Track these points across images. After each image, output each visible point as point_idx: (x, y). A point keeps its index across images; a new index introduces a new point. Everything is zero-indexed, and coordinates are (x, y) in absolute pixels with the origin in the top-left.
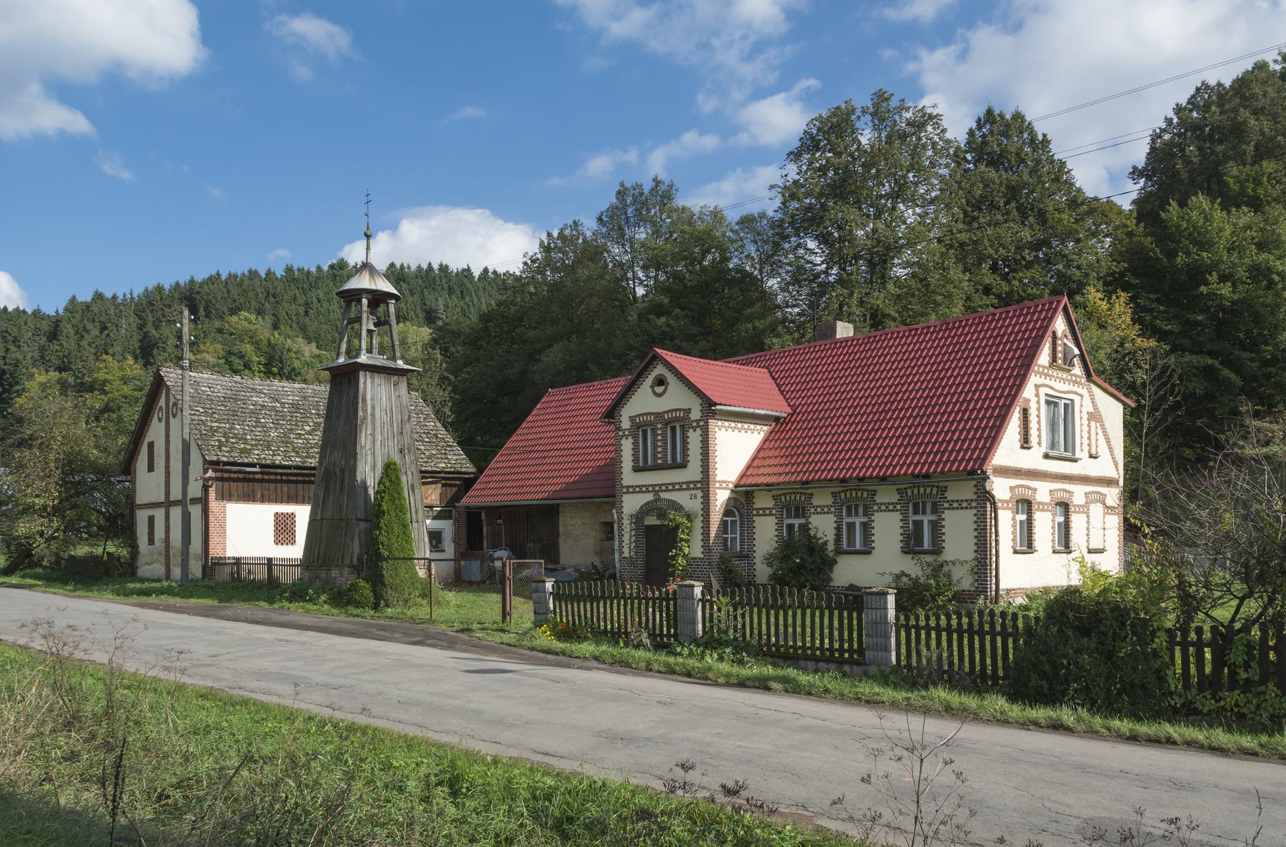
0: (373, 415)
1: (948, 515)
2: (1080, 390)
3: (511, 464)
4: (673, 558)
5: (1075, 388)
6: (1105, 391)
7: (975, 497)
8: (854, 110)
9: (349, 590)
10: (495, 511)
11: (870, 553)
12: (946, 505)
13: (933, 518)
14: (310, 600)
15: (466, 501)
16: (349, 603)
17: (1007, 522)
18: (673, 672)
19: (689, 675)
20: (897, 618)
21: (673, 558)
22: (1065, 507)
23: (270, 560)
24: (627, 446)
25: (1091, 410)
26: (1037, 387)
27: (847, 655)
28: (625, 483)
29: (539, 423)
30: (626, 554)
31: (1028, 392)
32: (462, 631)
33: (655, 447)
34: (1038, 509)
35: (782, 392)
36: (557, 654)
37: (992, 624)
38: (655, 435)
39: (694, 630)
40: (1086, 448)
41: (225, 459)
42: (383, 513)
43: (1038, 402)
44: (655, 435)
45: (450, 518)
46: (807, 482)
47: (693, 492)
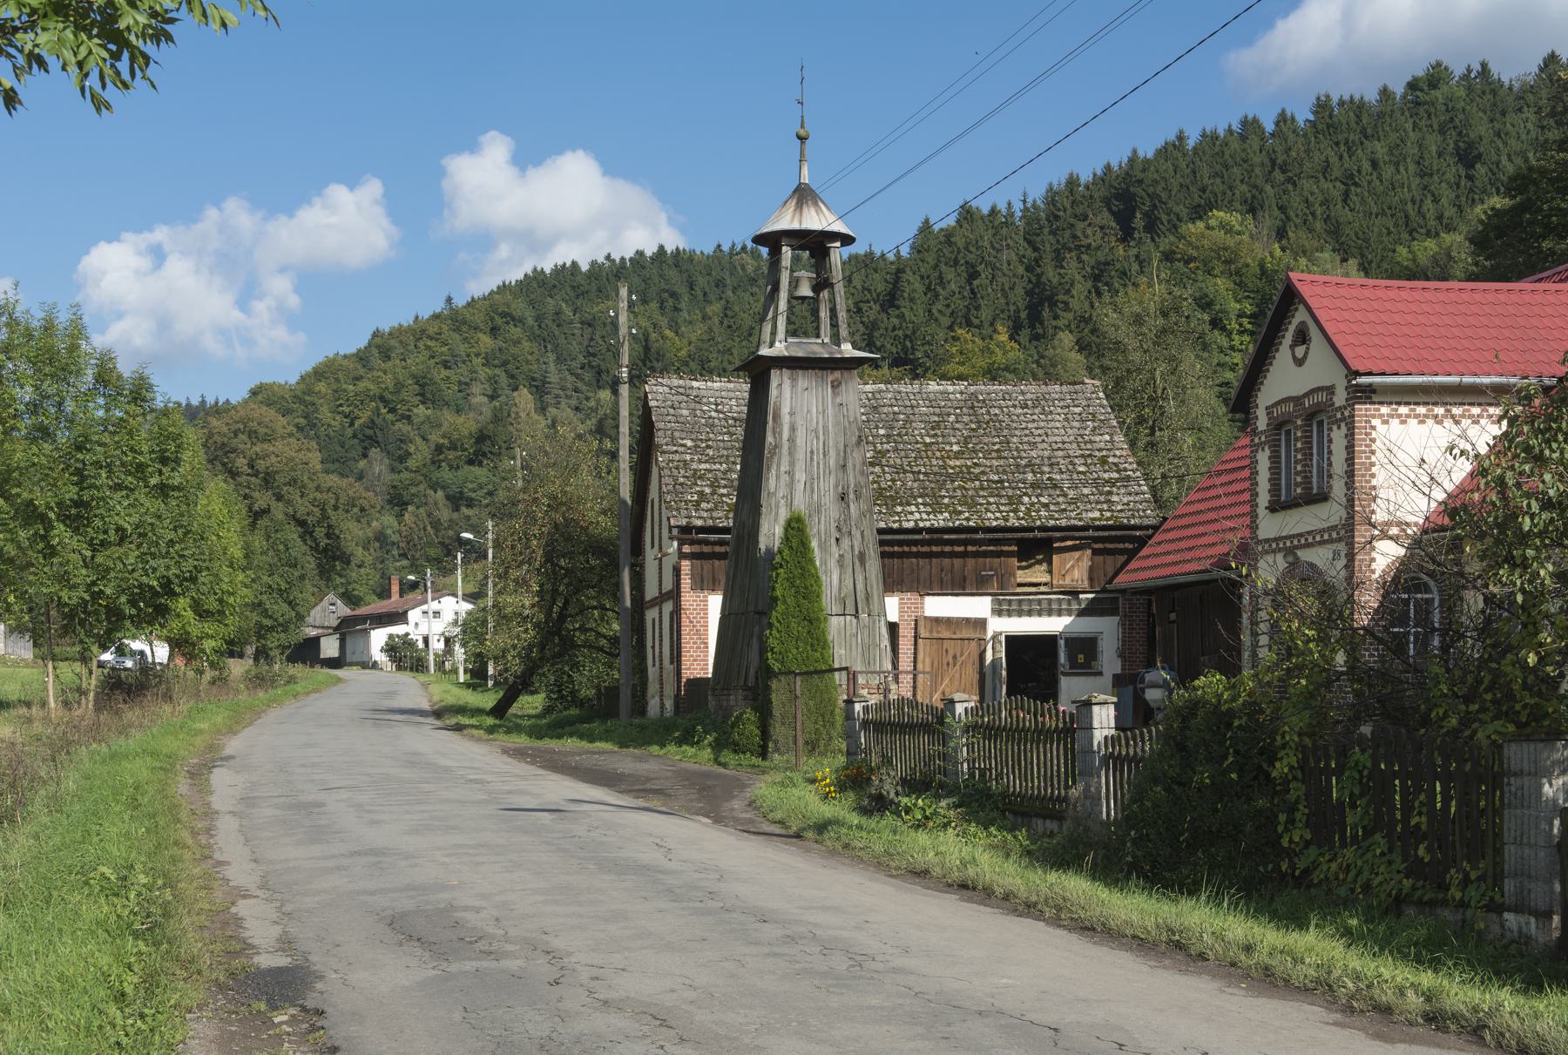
0: (792, 440)
41: (699, 523)
42: (775, 600)
45: (1112, 612)
47: (1335, 546)
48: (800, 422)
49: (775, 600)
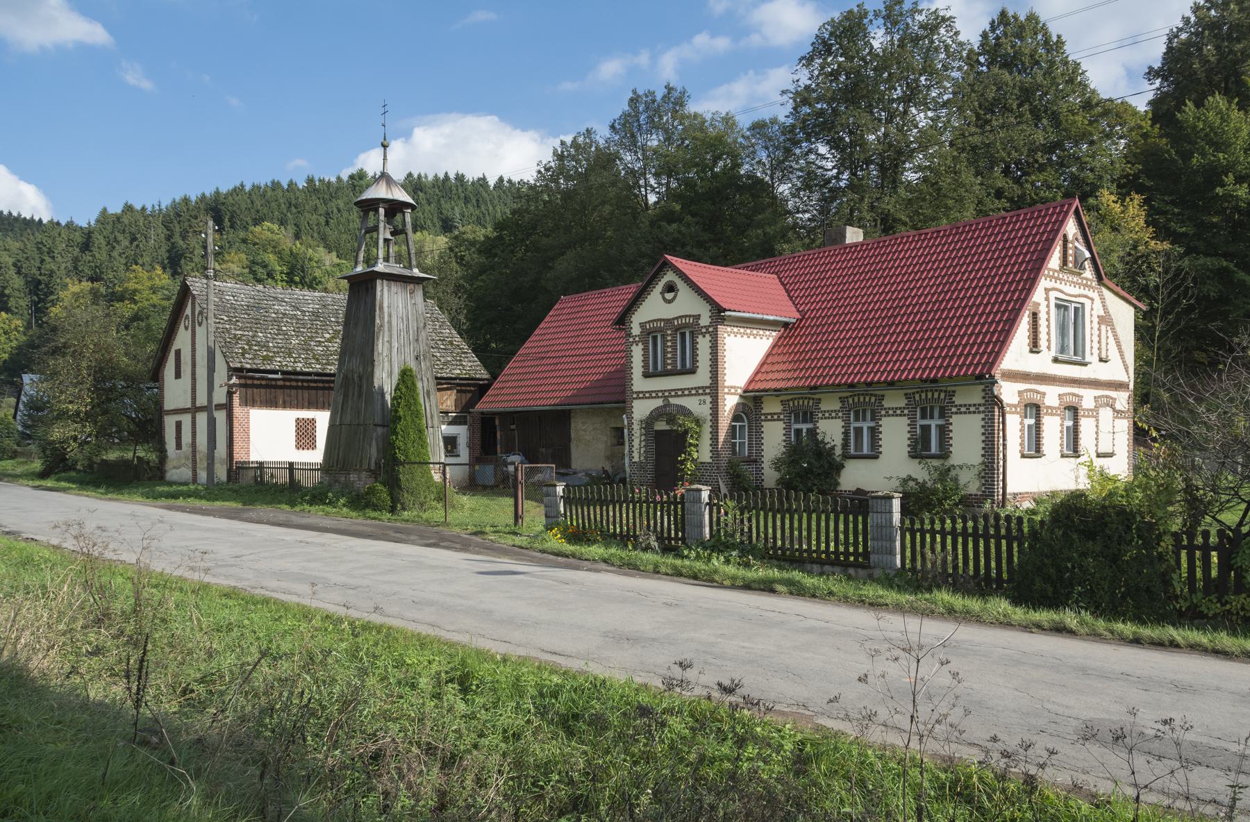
1: (955, 419)
2: (1090, 294)
3: (524, 370)
4: (682, 462)
5: (1086, 292)
6: (1116, 294)
7: (983, 401)
8: (866, 13)
9: (367, 493)
10: (510, 417)
11: (876, 457)
12: (954, 410)
13: (941, 422)
14: (330, 503)
15: (480, 407)
16: (367, 506)
17: (1015, 427)
18: (680, 574)
19: (695, 577)
20: (902, 521)
21: (682, 462)
22: (1074, 411)
23: (291, 464)
24: (637, 352)
25: (1102, 313)
26: (1047, 290)
27: (852, 559)
28: (635, 388)
29: (552, 330)
30: (636, 459)
31: (1038, 296)
32: (475, 534)
33: (664, 353)
34: (1047, 414)
35: (791, 298)
36: (567, 556)
37: (997, 527)
38: (664, 341)
39: (701, 533)
40: (1096, 352)
41: (248, 366)
42: (400, 418)
43: (1048, 306)
44: (664, 341)
45: (465, 423)
46: (815, 387)
47: (702, 398)
48: (394, 313)
49: (400, 418)
